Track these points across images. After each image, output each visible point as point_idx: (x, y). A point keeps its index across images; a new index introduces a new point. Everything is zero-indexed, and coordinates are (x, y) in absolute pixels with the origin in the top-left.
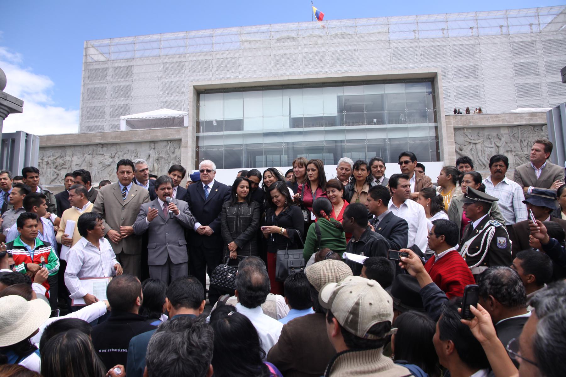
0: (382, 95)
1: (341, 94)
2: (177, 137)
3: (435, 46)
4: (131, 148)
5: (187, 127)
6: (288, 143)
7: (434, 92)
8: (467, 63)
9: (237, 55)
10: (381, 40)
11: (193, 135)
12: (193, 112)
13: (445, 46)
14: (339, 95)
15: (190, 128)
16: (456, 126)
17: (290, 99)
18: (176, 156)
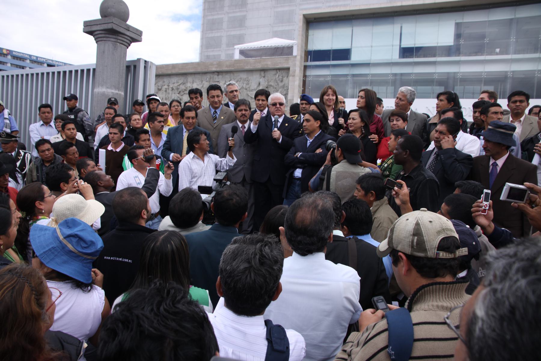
2: (286, 66)
4: (243, 76)
5: (296, 57)
6: (395, 75)
11: (301, 63)
12: (302, 41)
14: (457, 21)
15: (299, 57)
17: (401, 27)
18: (284, 85)
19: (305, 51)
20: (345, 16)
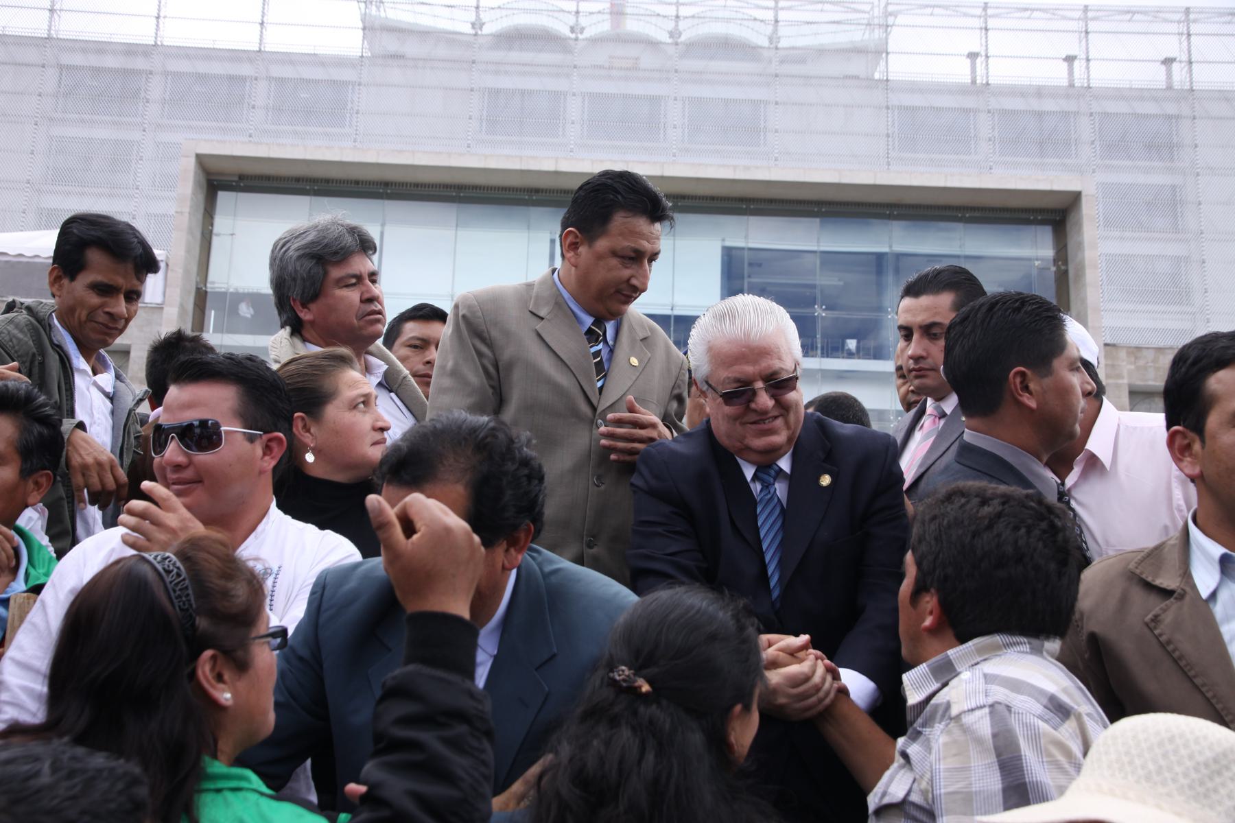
0: (880, 257)
1: (739, 243)
3: (1040, 115)
5: (159, 308)
7: (1066, 262)
8: (1149, 176)
9: (347, 75)
10: (857, 78)
12: (188, 251)
13: (1076, 114)
14: (729, 243)
16: (1139, 383)
19: (198, 290)
20: (357, 182)
